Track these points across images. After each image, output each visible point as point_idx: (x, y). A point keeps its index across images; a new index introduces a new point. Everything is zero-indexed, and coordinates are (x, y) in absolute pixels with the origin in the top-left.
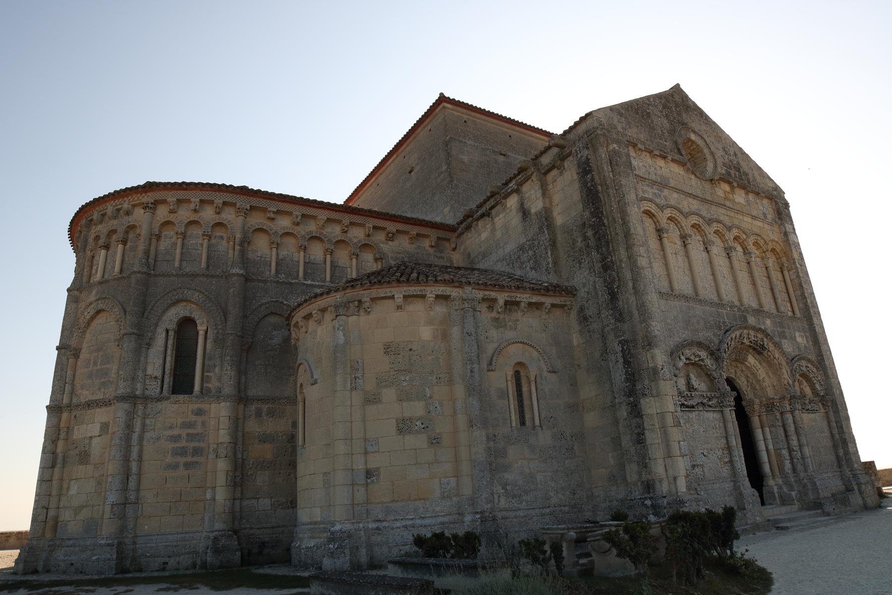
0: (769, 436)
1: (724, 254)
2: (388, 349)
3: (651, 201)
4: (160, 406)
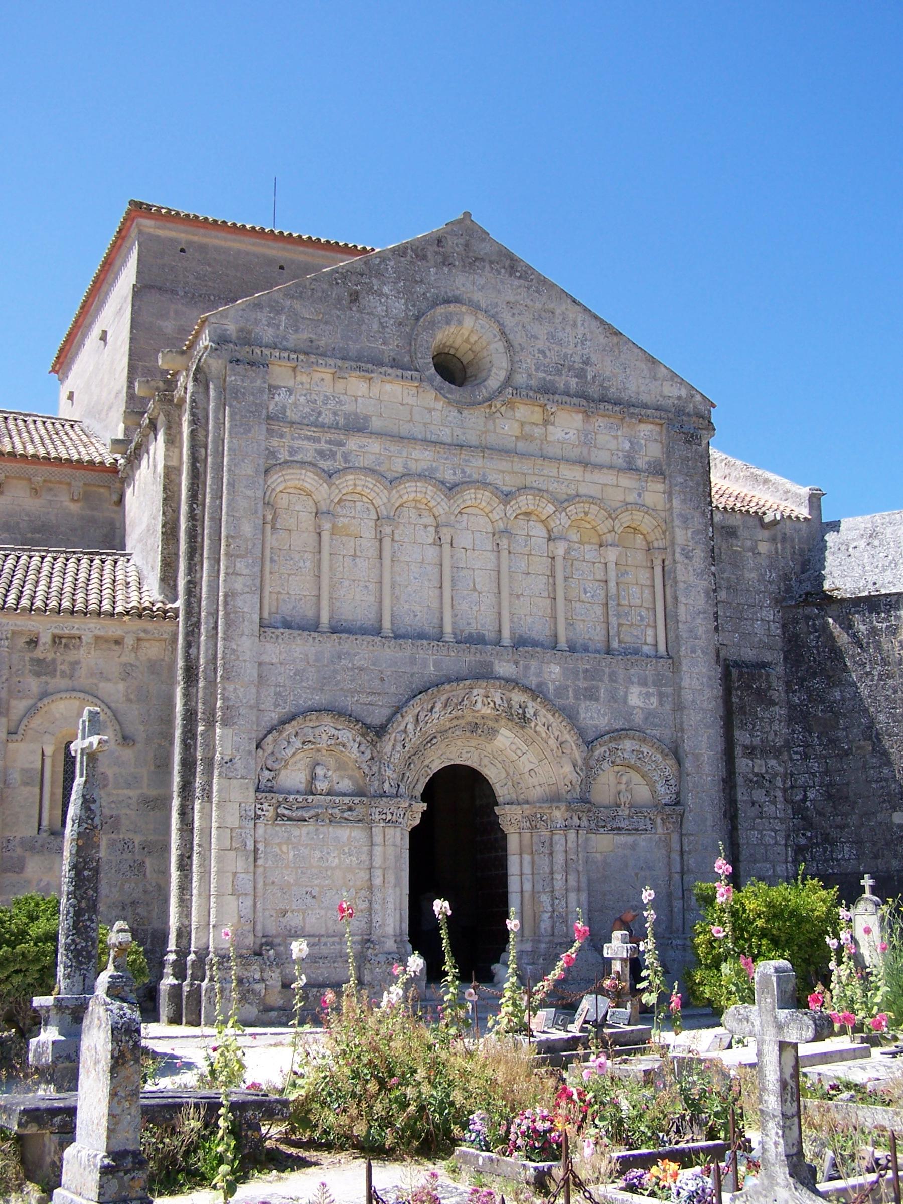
0: (527, 870)
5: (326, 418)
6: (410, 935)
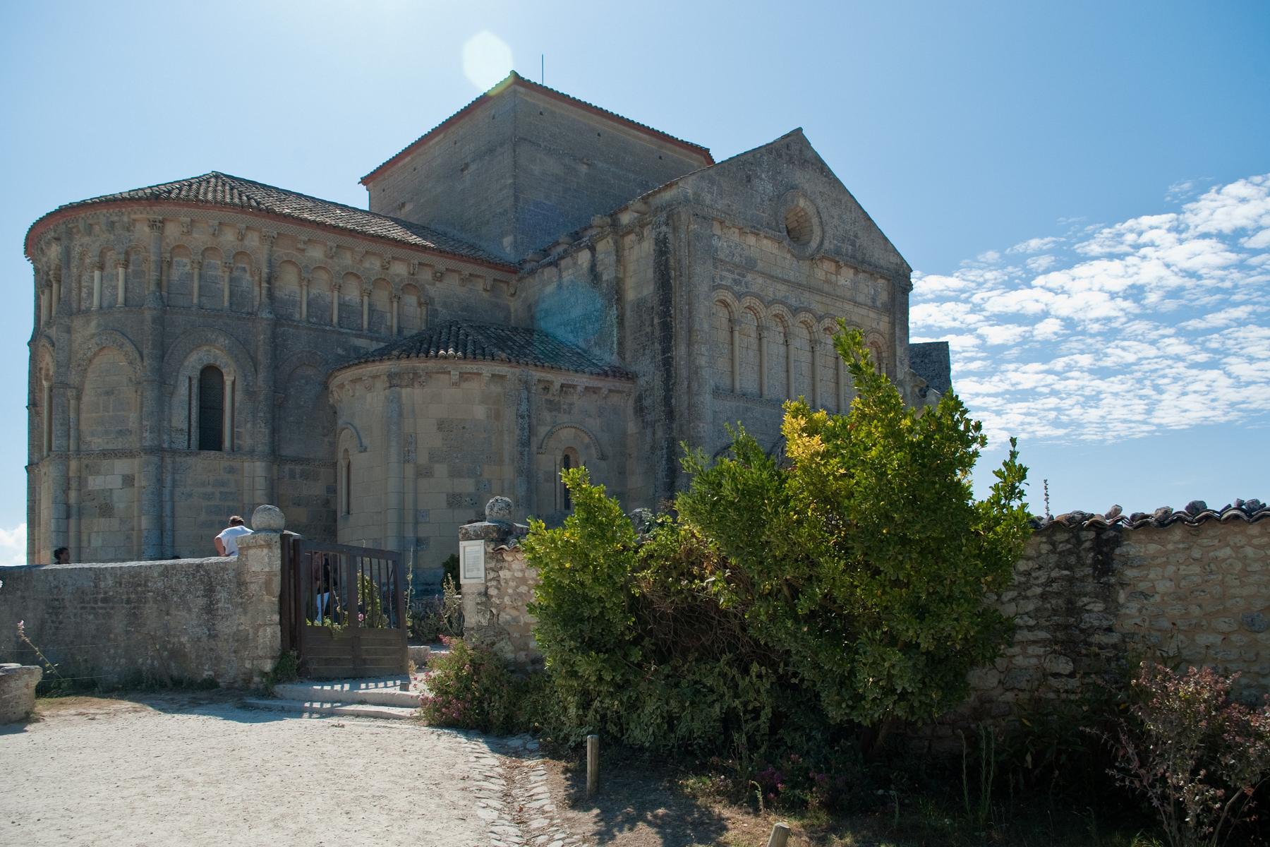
1: (808, 348)
2: (441, 425)
3: (727, 288)
4: (191, 460)
5: (737, 259)
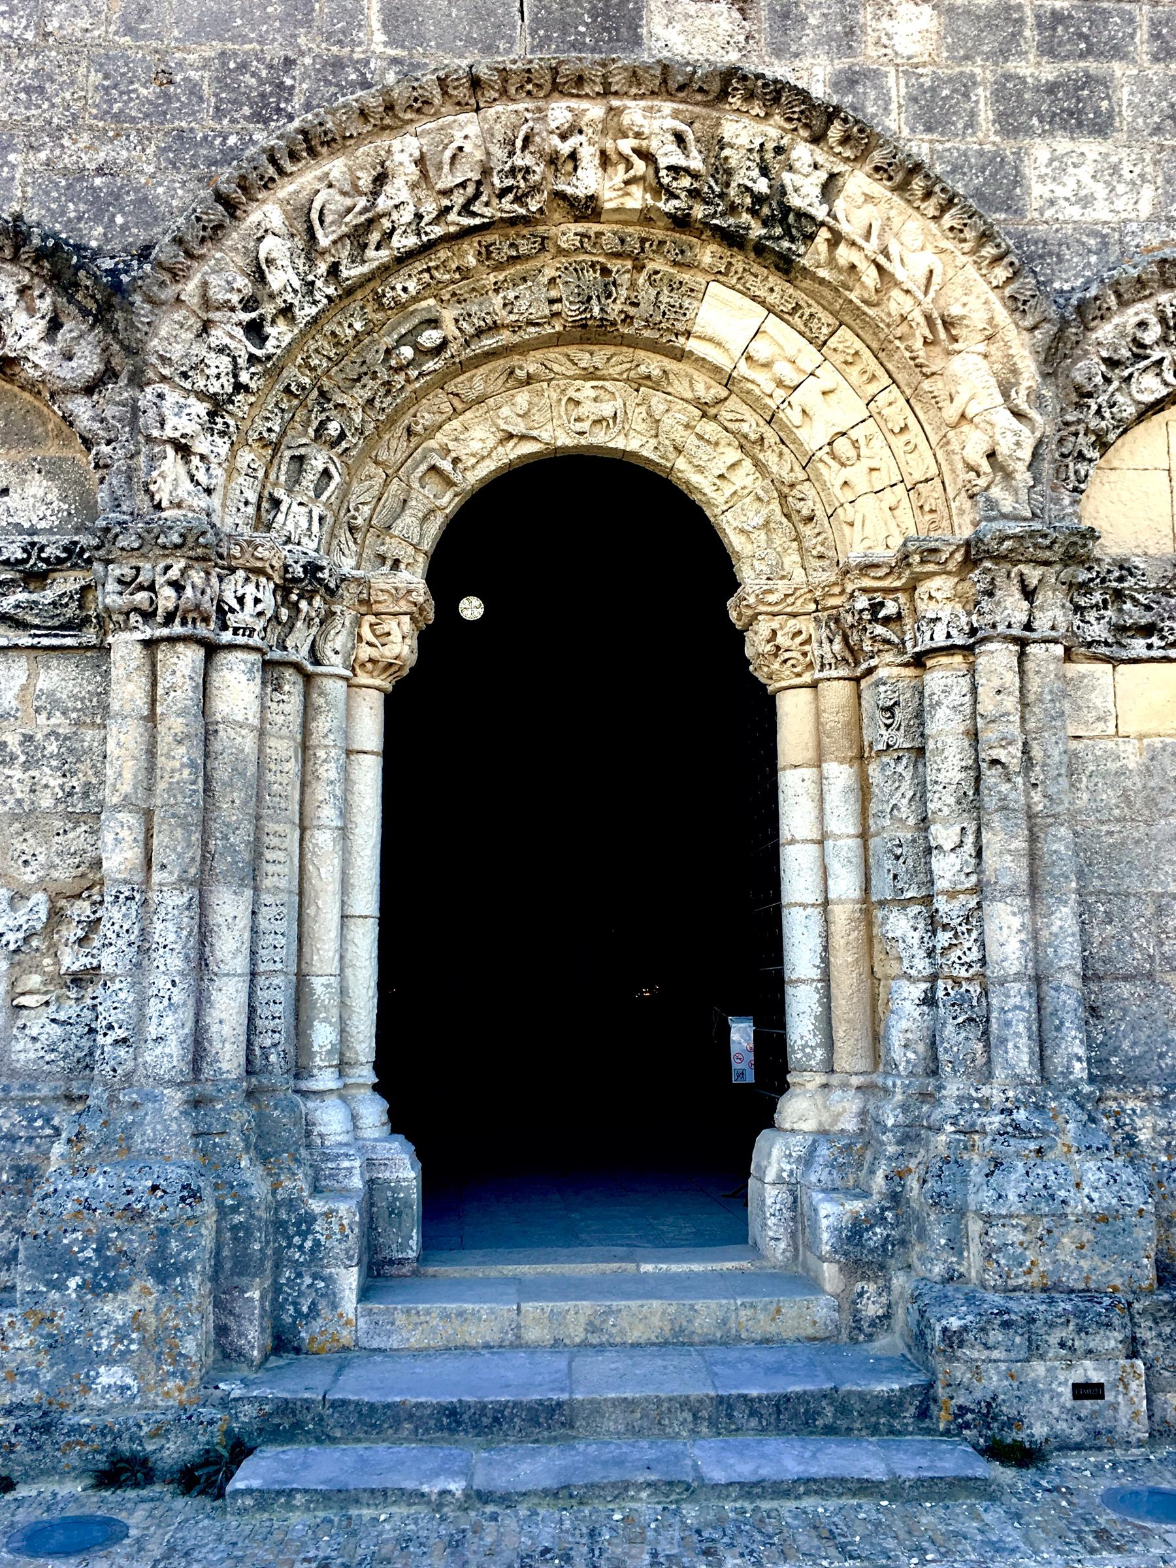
0: (842, 821)
6: (378, 1067)
